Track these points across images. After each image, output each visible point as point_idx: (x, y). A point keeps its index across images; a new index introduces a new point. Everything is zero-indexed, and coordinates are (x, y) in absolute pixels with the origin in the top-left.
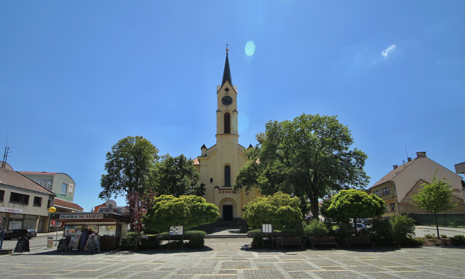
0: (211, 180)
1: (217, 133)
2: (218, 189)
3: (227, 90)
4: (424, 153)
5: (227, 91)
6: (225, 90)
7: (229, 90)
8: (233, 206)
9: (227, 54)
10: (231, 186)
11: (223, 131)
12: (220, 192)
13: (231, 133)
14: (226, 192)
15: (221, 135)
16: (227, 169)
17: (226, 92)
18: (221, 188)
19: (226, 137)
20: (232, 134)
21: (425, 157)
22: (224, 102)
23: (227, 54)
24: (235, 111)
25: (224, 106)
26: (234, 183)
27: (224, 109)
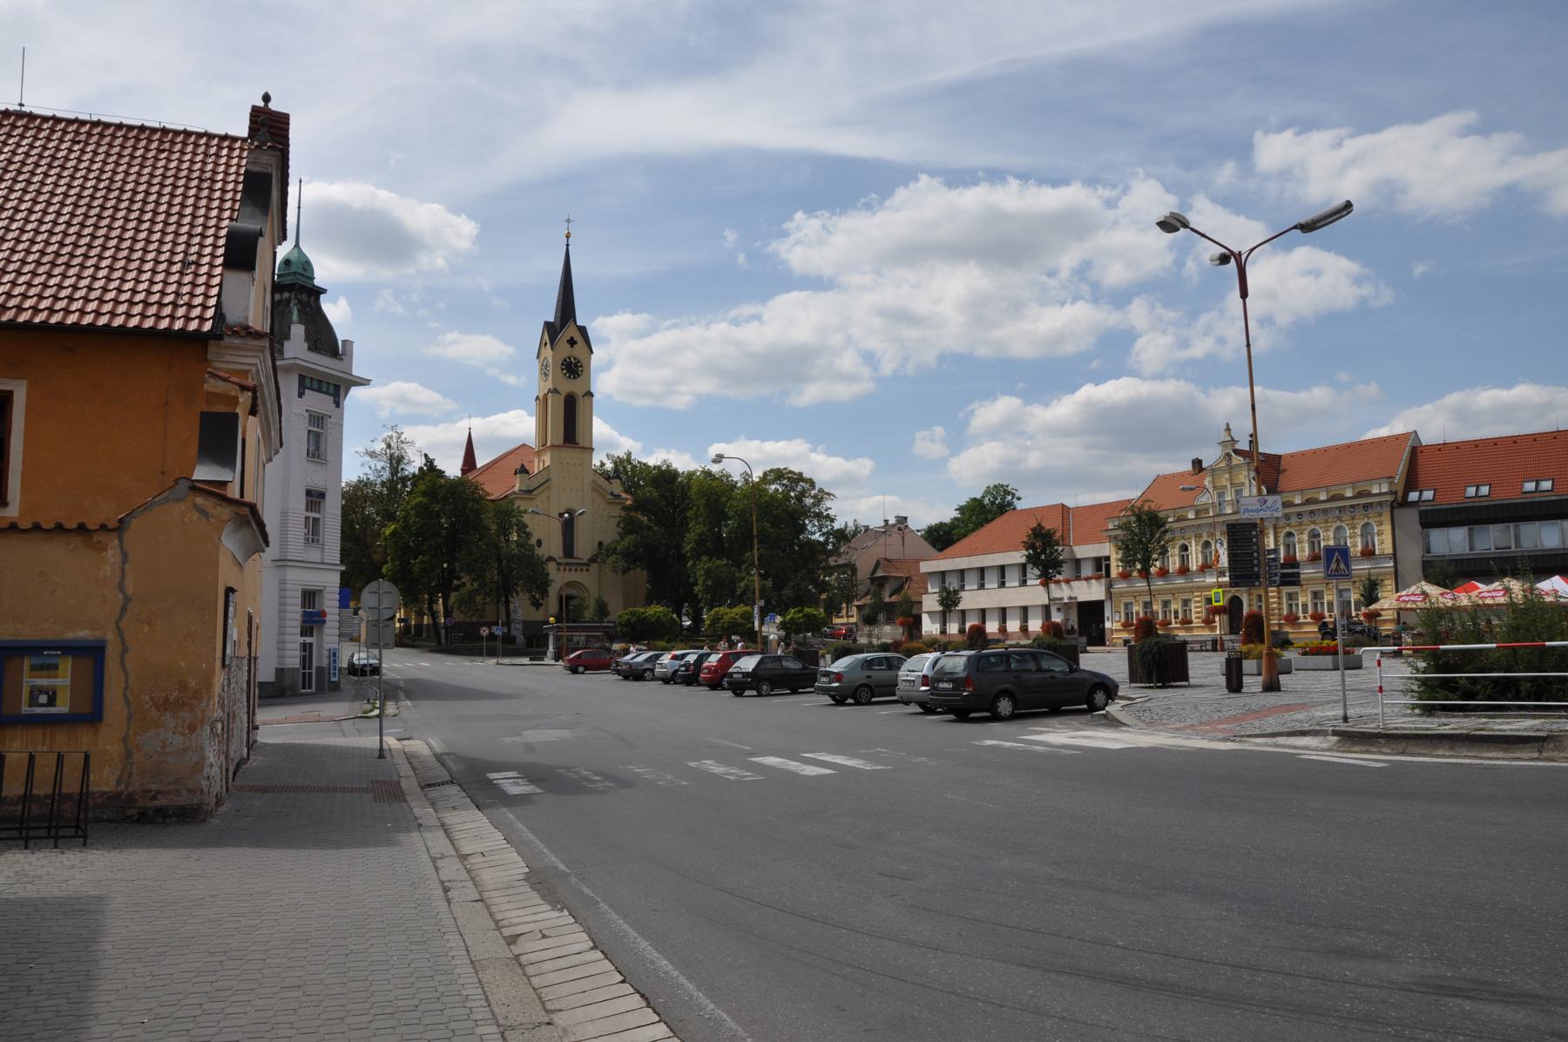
4: (906, 518)
5: (572, 346)
6: (568, 341)
7: (576, 343)
9: (568, 245)
10: (575, 556)
11: (560, 441)
12: (559, 570)
13: (578, 444)
14: (570, 570)
15: (560, 446)
18: (559, 561)
19: (569, 455)
20: (581, 445)
22: (565, 372)
23: (568, 245)
24: (590, 394)
27: (568, 386)
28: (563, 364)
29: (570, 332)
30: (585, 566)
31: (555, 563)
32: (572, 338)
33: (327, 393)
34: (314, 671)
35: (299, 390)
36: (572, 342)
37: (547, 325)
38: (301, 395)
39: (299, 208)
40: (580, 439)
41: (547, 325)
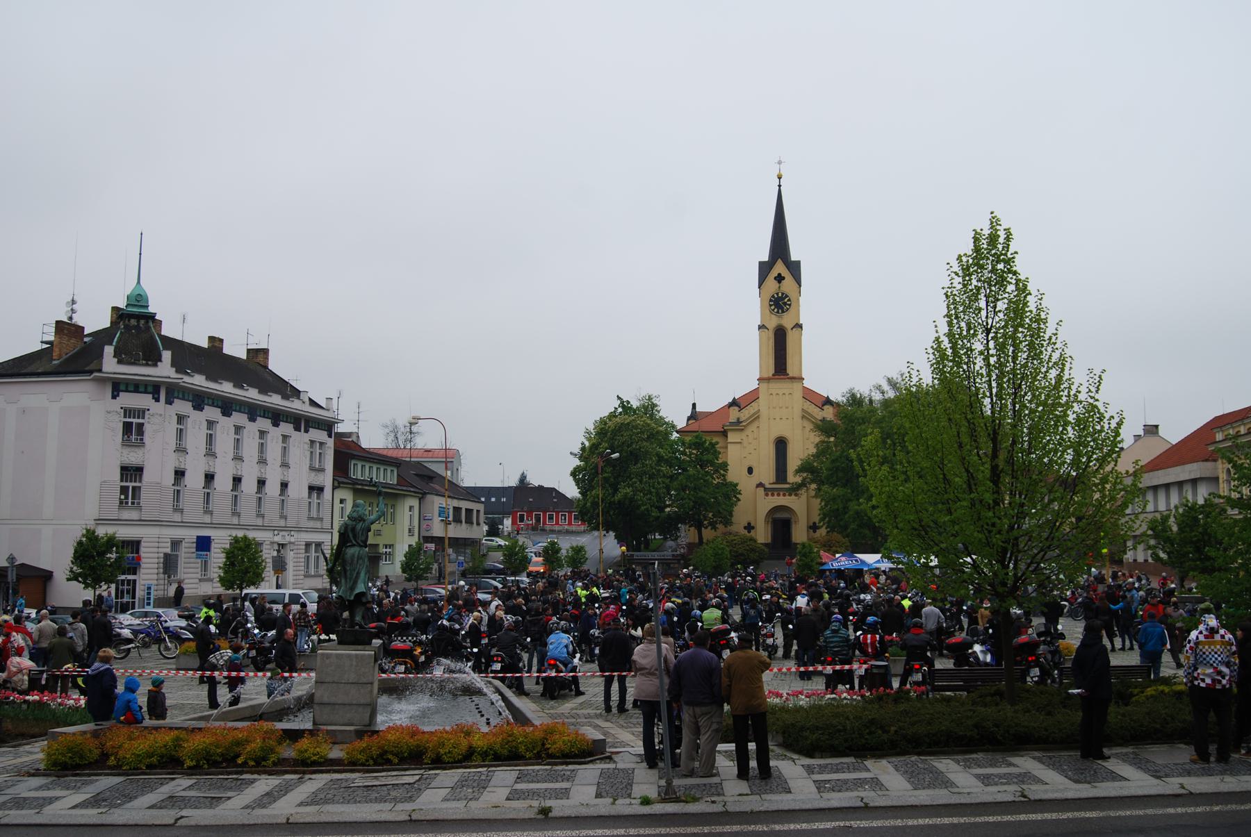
0: (750, 470)
1: (760, 372)
2: (762, 489)
3: (780, 278)
4: (1157, 426)
5: (779, 282)
6: (775, 278)
7: (784, 278)
8: (793, 520)
9: (780, 186)
11: (772, 371)
12: (767, 495)
16: (781, 445)
17: (778, 285)
18: (768, 486)
20: (791, 375)
21: (1157, 433)
23: (780, 186)
24: (799, 326)
25: (773, 316)
26: (793, 478)
28: (771, 300)
29: (779, 268)
30: (795, 490)
31: (762, 489)
32: (779, 274)
33: (146, 392)
34: (137, 600)
35: (113, 393)
36: (780, 278)
37: (761, 264)
38: (114, 397)
39: (140, 254)
40: (791, 371)
41: (761, 264)
